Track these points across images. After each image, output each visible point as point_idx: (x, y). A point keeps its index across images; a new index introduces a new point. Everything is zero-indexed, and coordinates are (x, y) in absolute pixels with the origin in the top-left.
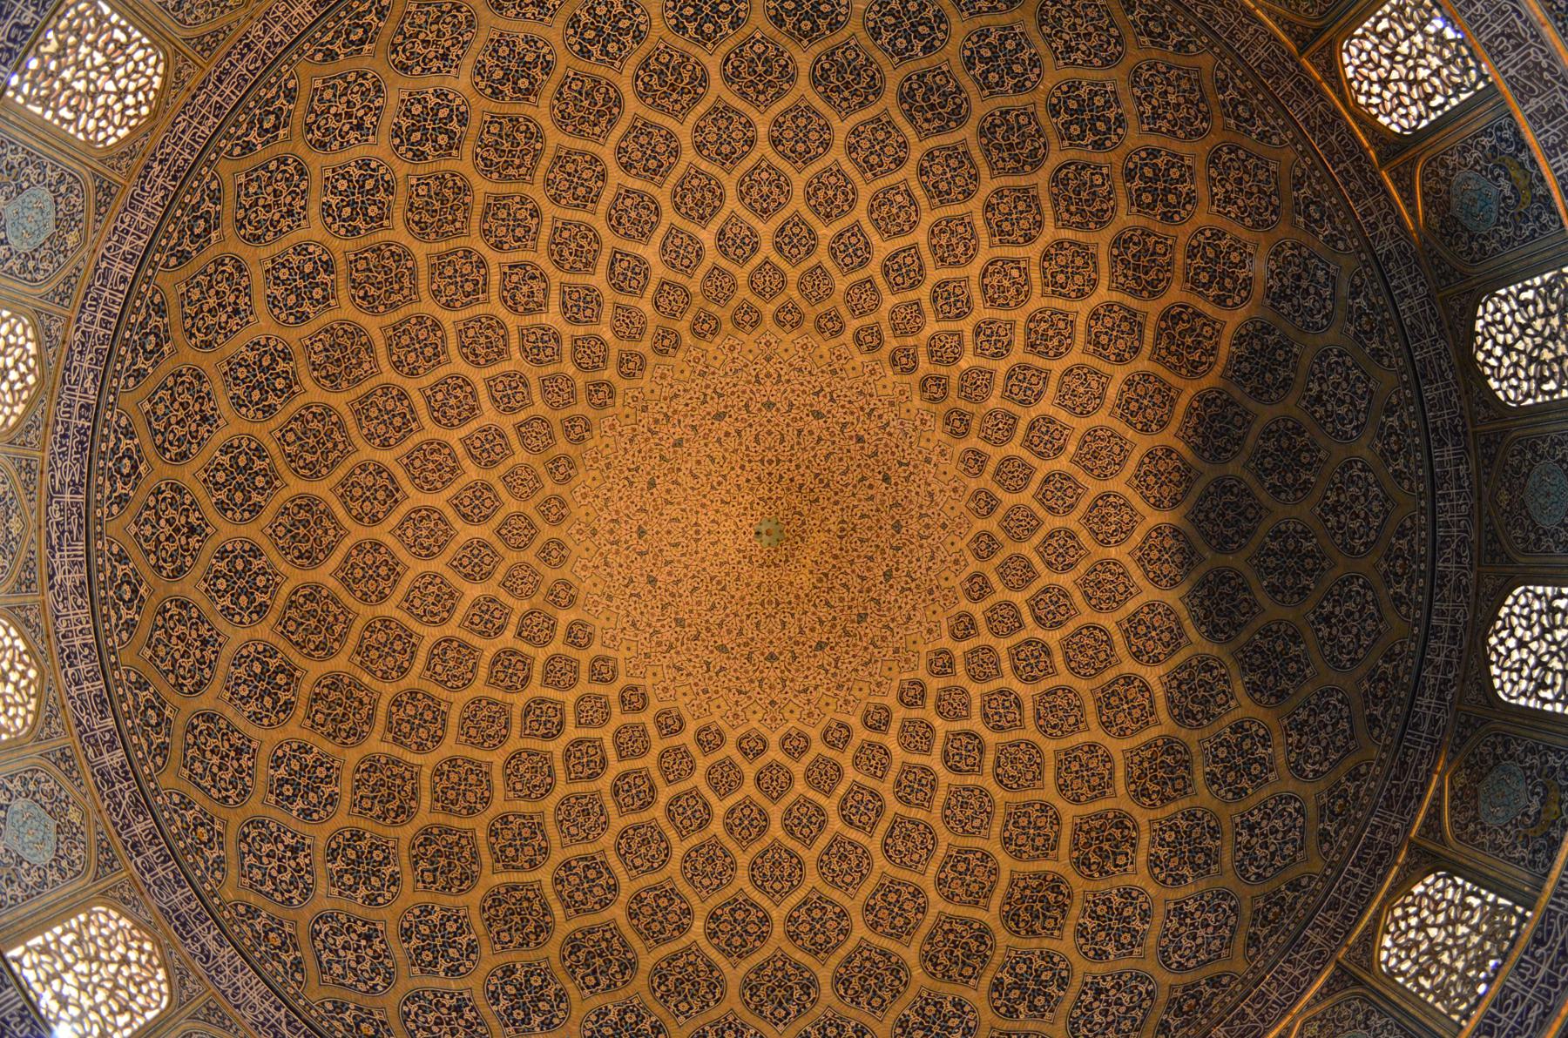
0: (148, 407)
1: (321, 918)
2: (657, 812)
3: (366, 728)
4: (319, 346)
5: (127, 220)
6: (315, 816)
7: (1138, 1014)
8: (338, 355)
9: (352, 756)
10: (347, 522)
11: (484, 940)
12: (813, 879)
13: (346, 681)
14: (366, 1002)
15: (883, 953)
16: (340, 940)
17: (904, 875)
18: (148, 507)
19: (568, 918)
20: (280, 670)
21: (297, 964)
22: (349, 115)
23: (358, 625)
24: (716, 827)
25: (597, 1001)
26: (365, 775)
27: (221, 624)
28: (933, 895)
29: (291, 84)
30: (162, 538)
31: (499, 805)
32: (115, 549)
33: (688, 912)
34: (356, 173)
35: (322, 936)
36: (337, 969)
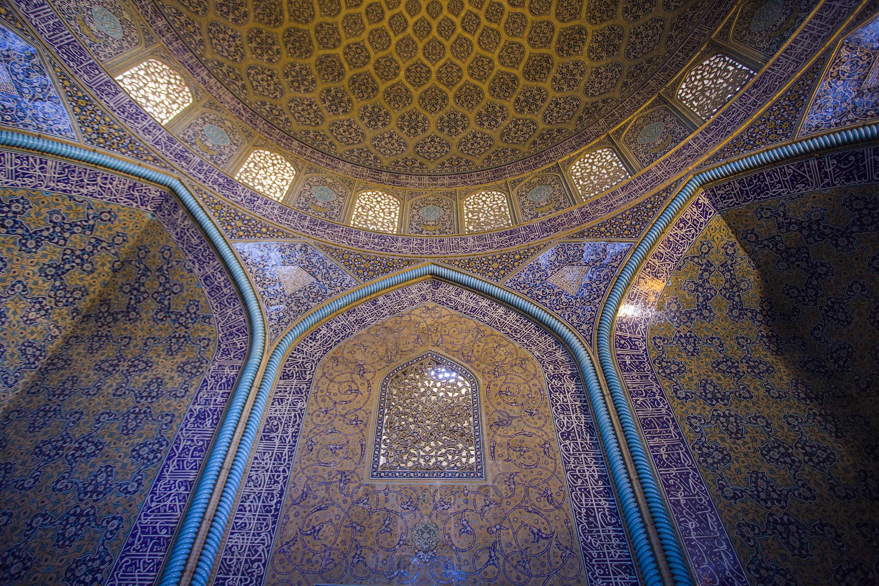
1: (250, 68)
2: (385, 23)
7: (571, 113)
11: (318, 78)
12: (448, 54)
14: (274, 102)
15: (474, 86)
17: (486, 54)
19: (351, 69)
21: (244, 86)
24: (410, 31)
25: (363, 103)
28: (496, 63)
31: (318, 19)
33: (398, 68)
36: (260, 89)
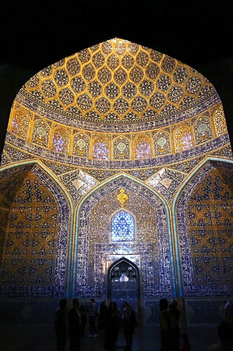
0: (102, 113)
3: (156, 66)
4: (88, 78)
5: (77, 126)
6: (170, 82)
8: (88, 73)
9: (161, 70)
10: (118, 67)
13: (147, 69)
16: (191, 87)
18: (118, 111)
20: (144, 84)
22: (49, 87)
23: (137, 65)
26: (165, 69)
27: (136, 96)
29: (49, 103)
30: (122, 108)
32: (124, 118)
34: (57, 80)
35: (189, 90)
36: (195, 90)
